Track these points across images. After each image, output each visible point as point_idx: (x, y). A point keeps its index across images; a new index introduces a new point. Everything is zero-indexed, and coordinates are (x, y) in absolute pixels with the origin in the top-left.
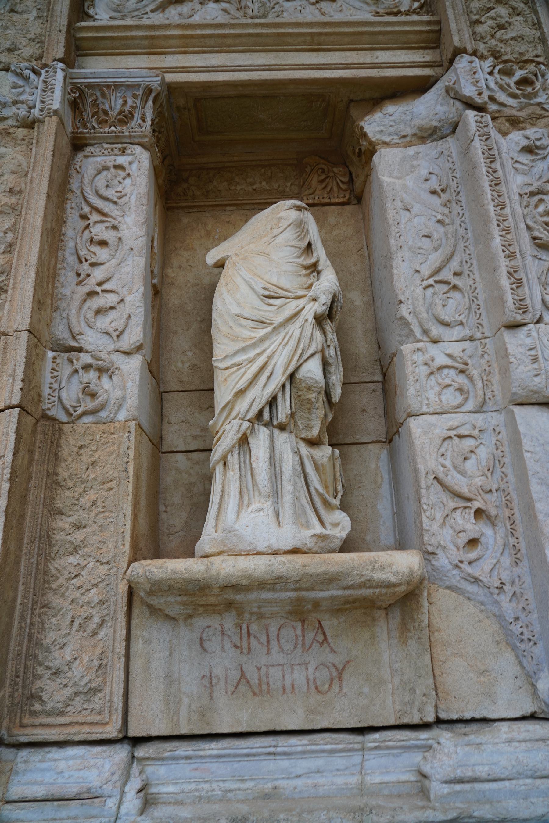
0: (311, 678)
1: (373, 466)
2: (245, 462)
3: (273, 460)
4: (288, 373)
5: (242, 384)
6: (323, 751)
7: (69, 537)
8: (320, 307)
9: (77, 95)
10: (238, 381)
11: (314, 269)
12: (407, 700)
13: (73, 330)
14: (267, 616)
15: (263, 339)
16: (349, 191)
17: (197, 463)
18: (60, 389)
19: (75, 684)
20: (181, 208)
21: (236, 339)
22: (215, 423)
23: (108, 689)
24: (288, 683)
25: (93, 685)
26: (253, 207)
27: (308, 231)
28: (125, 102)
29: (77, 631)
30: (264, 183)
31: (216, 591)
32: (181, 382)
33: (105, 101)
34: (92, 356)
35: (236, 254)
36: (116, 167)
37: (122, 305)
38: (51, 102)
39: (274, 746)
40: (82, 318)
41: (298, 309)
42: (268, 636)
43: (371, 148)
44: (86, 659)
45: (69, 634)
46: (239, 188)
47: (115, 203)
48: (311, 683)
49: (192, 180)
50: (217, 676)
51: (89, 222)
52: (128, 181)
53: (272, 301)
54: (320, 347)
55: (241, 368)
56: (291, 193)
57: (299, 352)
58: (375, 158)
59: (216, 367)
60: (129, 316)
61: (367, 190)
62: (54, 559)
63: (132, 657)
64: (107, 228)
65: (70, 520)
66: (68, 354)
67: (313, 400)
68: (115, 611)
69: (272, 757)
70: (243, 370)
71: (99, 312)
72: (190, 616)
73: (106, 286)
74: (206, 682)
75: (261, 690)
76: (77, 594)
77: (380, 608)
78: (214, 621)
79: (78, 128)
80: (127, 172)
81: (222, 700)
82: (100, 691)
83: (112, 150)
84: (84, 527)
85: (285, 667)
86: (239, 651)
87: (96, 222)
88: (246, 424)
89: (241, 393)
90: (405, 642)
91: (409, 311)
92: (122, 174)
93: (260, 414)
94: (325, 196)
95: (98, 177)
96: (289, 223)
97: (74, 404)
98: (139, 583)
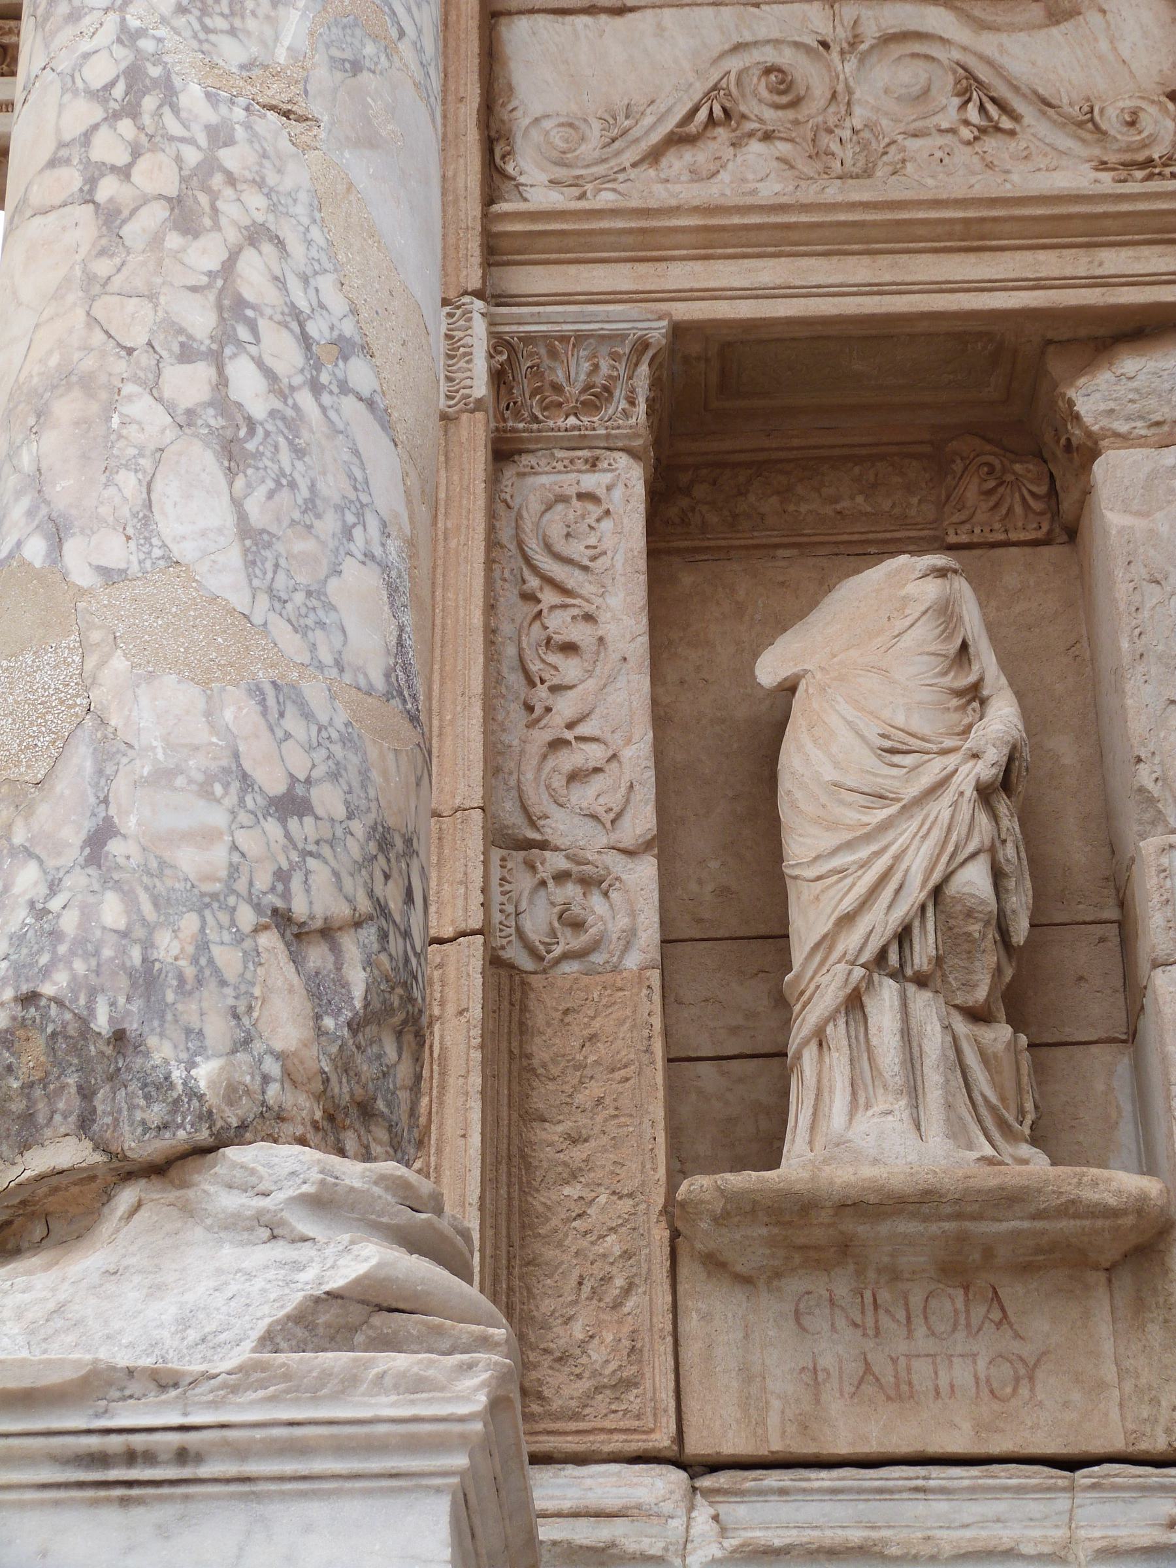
0: (982, 1376)
1: (1100, 1087)
2: (857, 1038)
3: (907, 1034)
4: (931, 884)
5: (847, 904)
6: (1006, 1489)
7: (561, 1155)
8: (986, 769)
9: (505, 357)
10: (841, 900)
11: (974, 696)
12: (1145, 1415)
13: (531, 810)
14: (907, 1276)
15: (885, 826)
16: (1049, 515)
17: (741, 1080)
18: (517, 915)
19: (595, 1374)
20: (678, 551)
21: (832, 826)
22: (798, 977)
23: (648, 1384)
24: (943, 1382)
25: (625, 1374)
26: (836, 550)
27: (961, 618)
28: (596, 367)
29: (589, 1299)
30: (860, 499)
31: (825, 1216)
32: (700, 921)
33: (557, 364)
34: (567, 857)
35: (822, 669)
36: (581, 496)
37: (614, 765)
38: (468, 382)
39: (924, 1478)
40: (542, 788)
41: (945, 773)
42: (908, 1310)
43: (1089, 444)
44: (609, 1338)
45: (576, 1302)
46: (804, 508)
47: (585, 569)
48: (983, 1383)
49: (700, 491)
50: (824, 1370)
51: (540, 607)
52: (606, 525)
53: (897, 759)
54: (987, 843)
55: (845, 877)
56: (919, 520)
57: (950, 848)
58: (1099, 467)
59: (796, 878)
60: (631, 786)
61: (1084, 522)
62: (538, 1191)
63: (682, 1341)
64: (574, 618)
65: (560, 1128)
66: (523, 853)
67: (977, 935)
68: (649, 1269)
69: (920, 1496)
70: (849, 881)
71: (574, 777)
72: (778, 1275)
73: (583, 730)
74: (807, 1377)
75: (901, 1394)
76: (584, 1243)
77: (1096, 1267)
78: (818, 1284)
79: (505, 420)
80: (605, 506)
81: (835, 1405)
82: (636, 1385)
83: (572, 462)
84: (586, 1140)
85: (939, 1359)
86: (860, 1332)
87: (553, 608)
88: (859, 972)
89: (847, 920)
90: (1142, 1328)
91: (1154, 776)
92: (595, 511)
93: (882, 955)
94: (997, 526)
95: (548, 516)
96: (923, 608)
97: (547, 940)
98: (702, 1202)
